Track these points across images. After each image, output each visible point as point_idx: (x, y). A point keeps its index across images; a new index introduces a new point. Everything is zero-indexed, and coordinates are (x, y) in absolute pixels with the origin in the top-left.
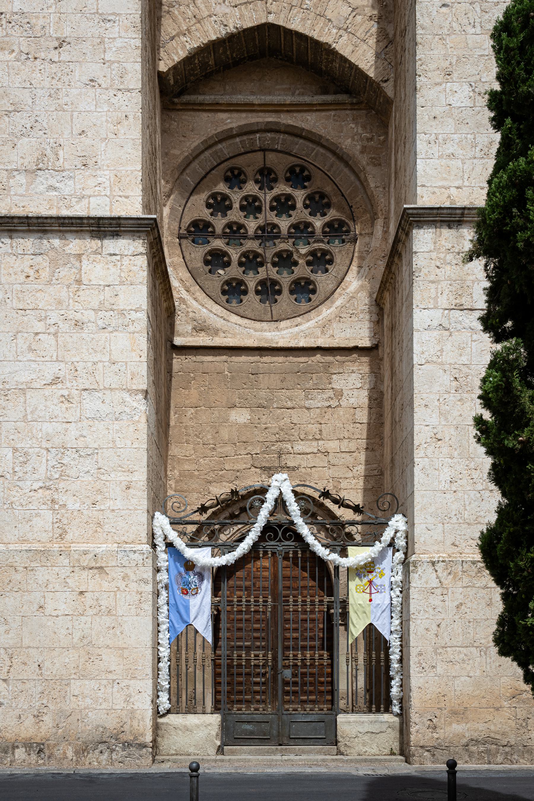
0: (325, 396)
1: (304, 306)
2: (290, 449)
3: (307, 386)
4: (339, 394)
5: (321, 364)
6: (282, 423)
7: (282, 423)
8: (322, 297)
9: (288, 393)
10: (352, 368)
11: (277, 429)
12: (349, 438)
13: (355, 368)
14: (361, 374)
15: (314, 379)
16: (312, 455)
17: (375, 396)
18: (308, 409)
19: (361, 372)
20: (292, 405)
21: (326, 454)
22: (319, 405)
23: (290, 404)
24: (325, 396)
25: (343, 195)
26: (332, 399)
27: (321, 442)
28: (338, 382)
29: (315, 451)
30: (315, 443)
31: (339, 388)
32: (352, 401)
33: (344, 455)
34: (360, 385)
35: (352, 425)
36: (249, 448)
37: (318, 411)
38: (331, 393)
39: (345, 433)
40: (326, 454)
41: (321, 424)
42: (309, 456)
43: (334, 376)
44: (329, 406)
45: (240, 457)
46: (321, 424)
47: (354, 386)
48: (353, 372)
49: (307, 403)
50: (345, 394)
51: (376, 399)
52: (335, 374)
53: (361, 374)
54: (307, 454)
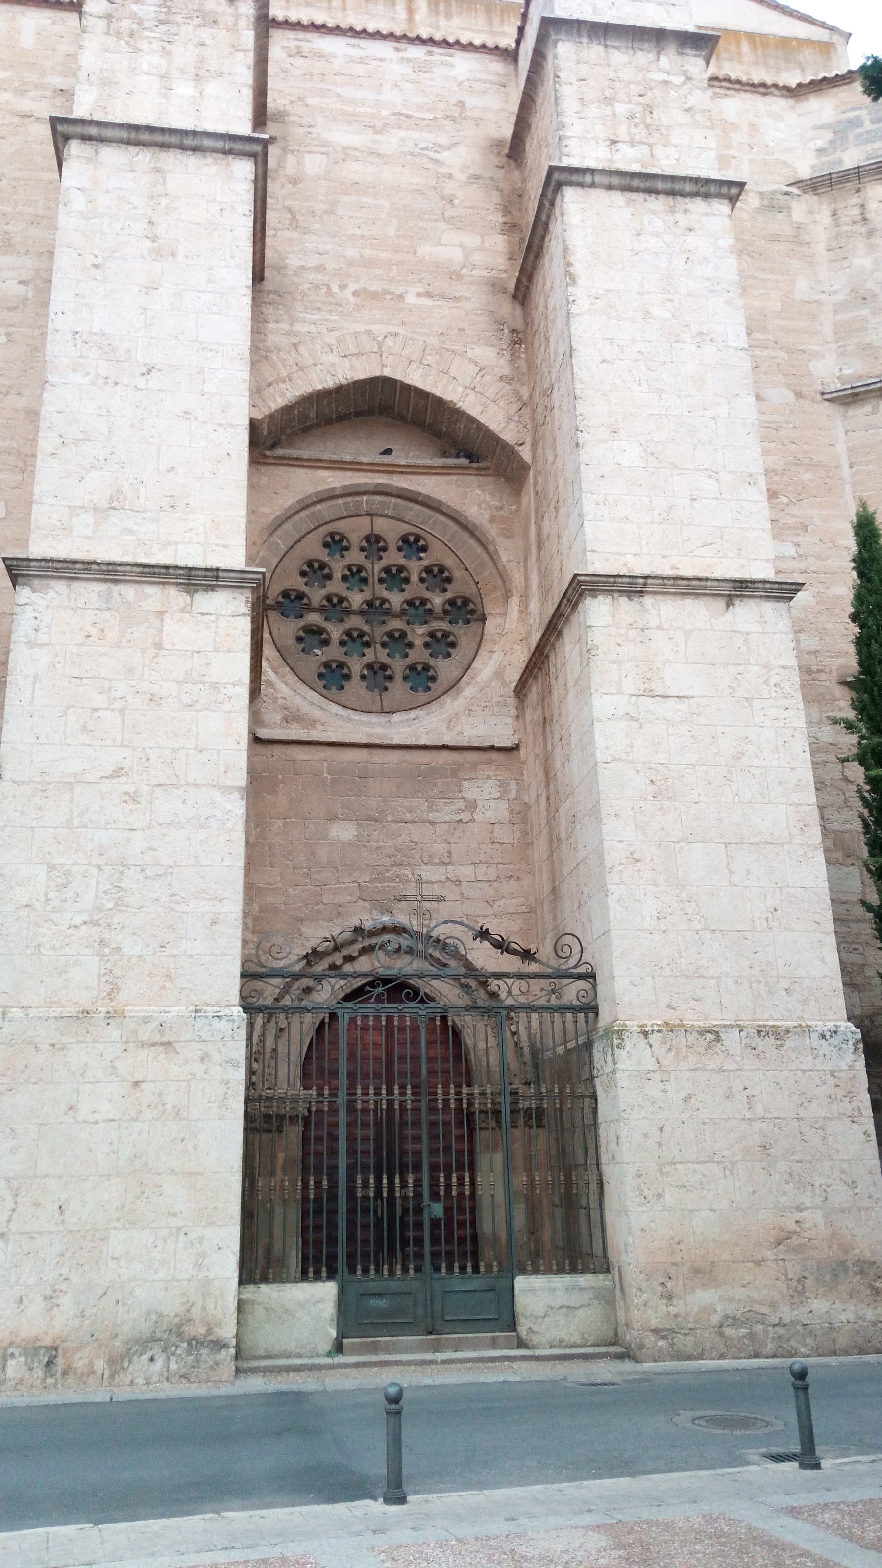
0: (454, 808)
1: (422, 697)
2: (410, 876)
4: (472, 806)
6: (399, 841)
7: (399, 841)
8: (446, 686)
9: (406, 803)
10: (487, 773)
11: (393, 850)
12: (486, 863)
13: (491, 773)
14: (499, 780)
15: (439, 785)
16: (438, 884)
17: (518, 808)
18: (433, 823)
19: (499, 778)
20: (412, 819)
21: (458, 883)
22: (447, 819)
23: (408, 817)
25: (467, 570)
26: (463, 811)
27: (450, 868)
28: (470, 791)
29: (443, 878)
30: (442, 869)
31: (471, 797)
32: (489, 814)
33: (480, 885)
34: (498, 795)
36: (355, 874)
37: (445, 826)
38: (461, 804)
39: (482, 855)
40: (458, 883)
41: (449, 843)
42: (435, 886)
43: (465, 783)
44: (460, 821)
45: (343, 886)
46: (449, 843)
47: (491, 796)
48: (488, 778)
49: (432, 816)
51: (520, 813)
52: (466, 779)
53: (499, 780)
54: (433, 883)
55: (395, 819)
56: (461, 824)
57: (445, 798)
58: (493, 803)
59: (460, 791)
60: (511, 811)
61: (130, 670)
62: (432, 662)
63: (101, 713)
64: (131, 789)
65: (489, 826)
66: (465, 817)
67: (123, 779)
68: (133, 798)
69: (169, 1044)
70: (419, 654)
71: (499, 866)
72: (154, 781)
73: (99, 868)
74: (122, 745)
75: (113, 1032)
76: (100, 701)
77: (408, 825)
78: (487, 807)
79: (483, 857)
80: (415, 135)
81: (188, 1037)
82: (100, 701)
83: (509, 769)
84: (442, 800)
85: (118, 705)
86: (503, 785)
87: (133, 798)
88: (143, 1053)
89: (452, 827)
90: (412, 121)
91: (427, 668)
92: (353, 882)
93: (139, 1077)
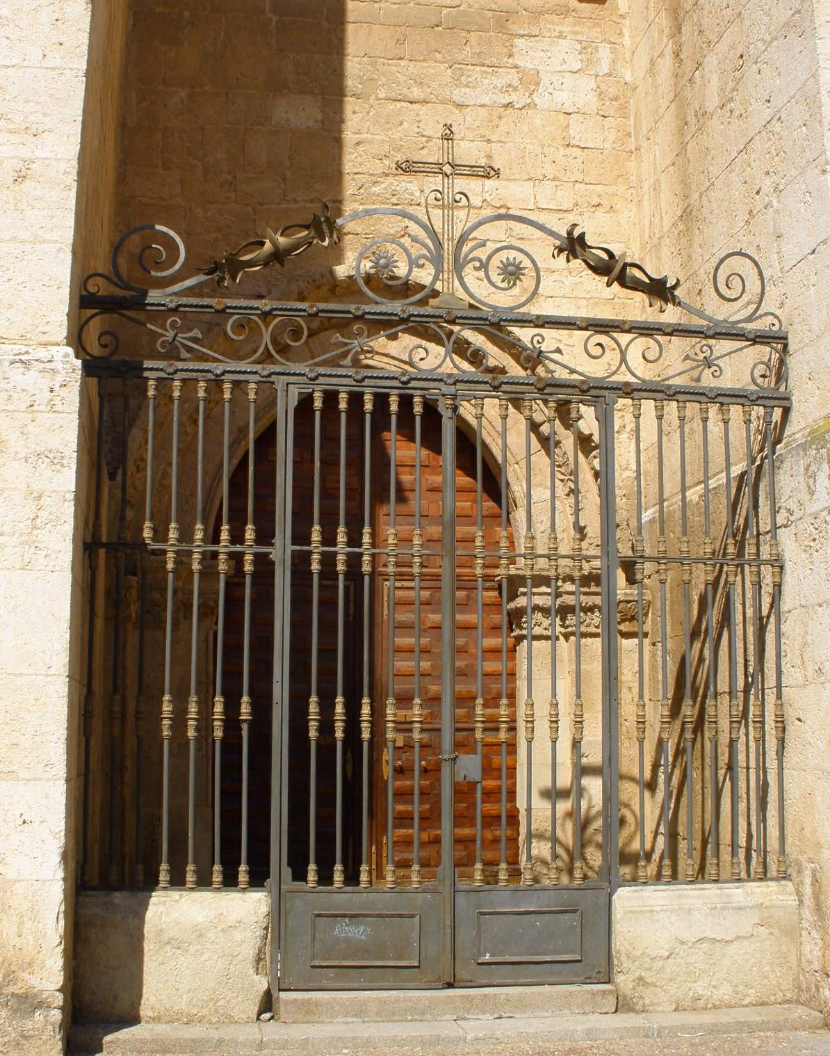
0: (499, 82)
2: (417, 194)
3: (459, 57)
4: (531, 81)
5: (490, 14)
6: (397, 134)
7: (397, 134)
9: (413, 68)
10: (559, 28)
11: (386, 147)
12: (556, 178)
13: (566, 29)
18: (459, 106)
19: (580, 37)
20: (422, 96)
22: (486, 100)
23: (416, 93)
24: (499, 82)
26: (515, 89)
28: (528, 54)
31: (529, 66)
32: (561, 97)
34: (578, 66)
35: (562, 151)
36: (317, 186)
37: (483, 112)
38: (512, 77)
39: (547, 166)
41: (489, 141)
43: (519, 42)
45: (294, 206)
46: (489, 141)
47: (564, 67)
48: (561, 36)
49: (458, 95)
50: (545, 79)
51: (616, 99)
53: (580, 42)
55: (393, 95)
56: (510, 110)
57: (483, 65)
58: (569, 80)
59: (510, 56)
60: (601, 95)
65: (562, 117)
66: (519, 99)
71: (577, 185)
77: (414, 106)
78: (557, 85)
79: (550, 171)
83: (598, 25)
84: (478, 68)
86: (587, 49)
89: (495, 113)
92: (312, 201)
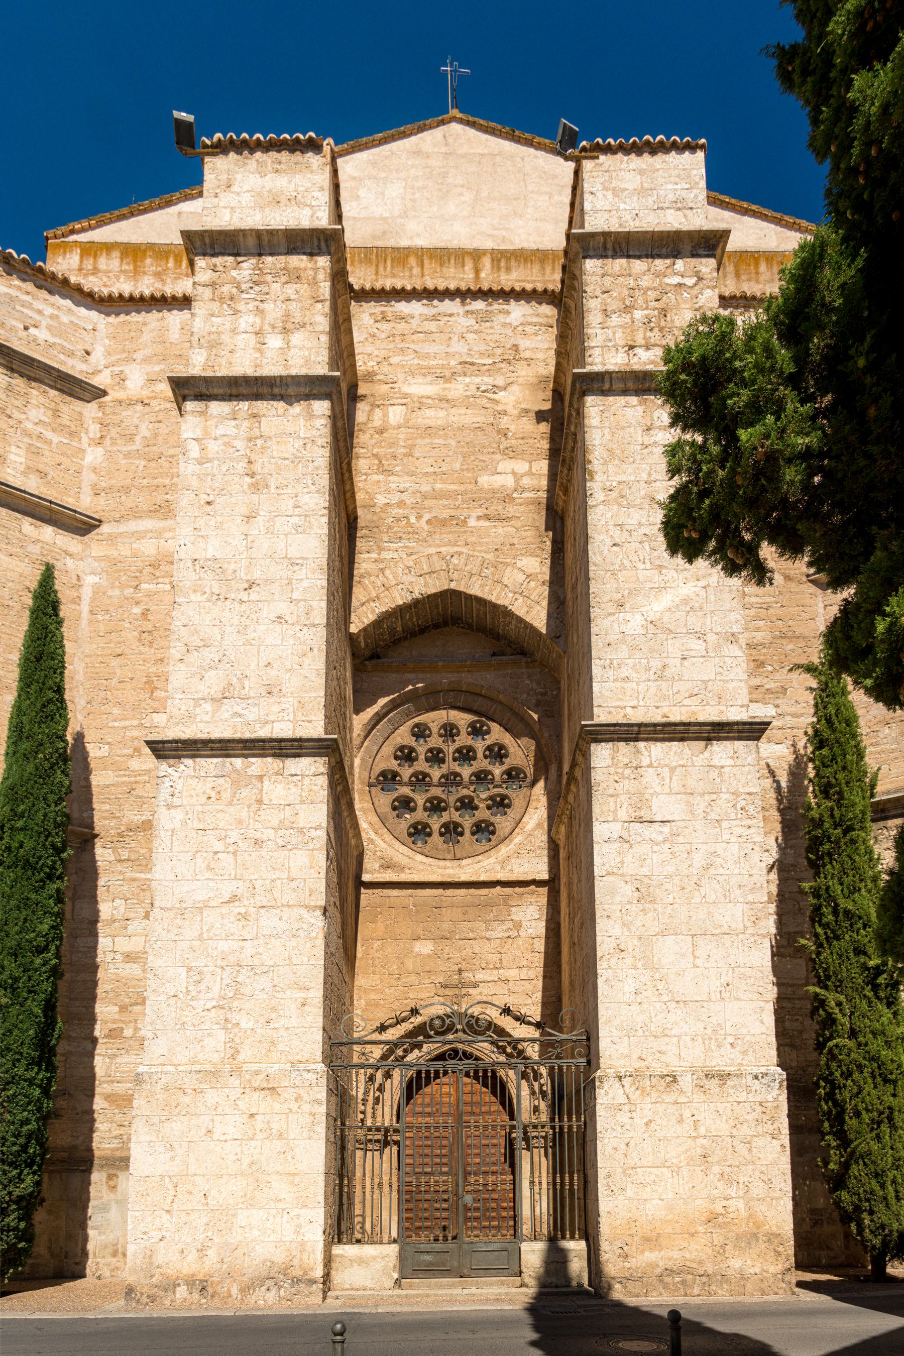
61: (240, 822)
62: (492, 819)
63: (219, 855)
64: (243, 910)
67: (237, 904)
68: (244, 917)
69: (273, 1088)
70: (482, 813)
72: (259, 904)
73: (222, 968)
74: (235, 879)
75: (235, 1082)
76: (219, 846)
80: (477, 380)
81: (286, 1084)
82: (219, 846)
85: (231, 849)
87: (244, 917)
88: (256, 1095)
90: (475, 368)
91: (489, 824)
93: (253, 1111)
